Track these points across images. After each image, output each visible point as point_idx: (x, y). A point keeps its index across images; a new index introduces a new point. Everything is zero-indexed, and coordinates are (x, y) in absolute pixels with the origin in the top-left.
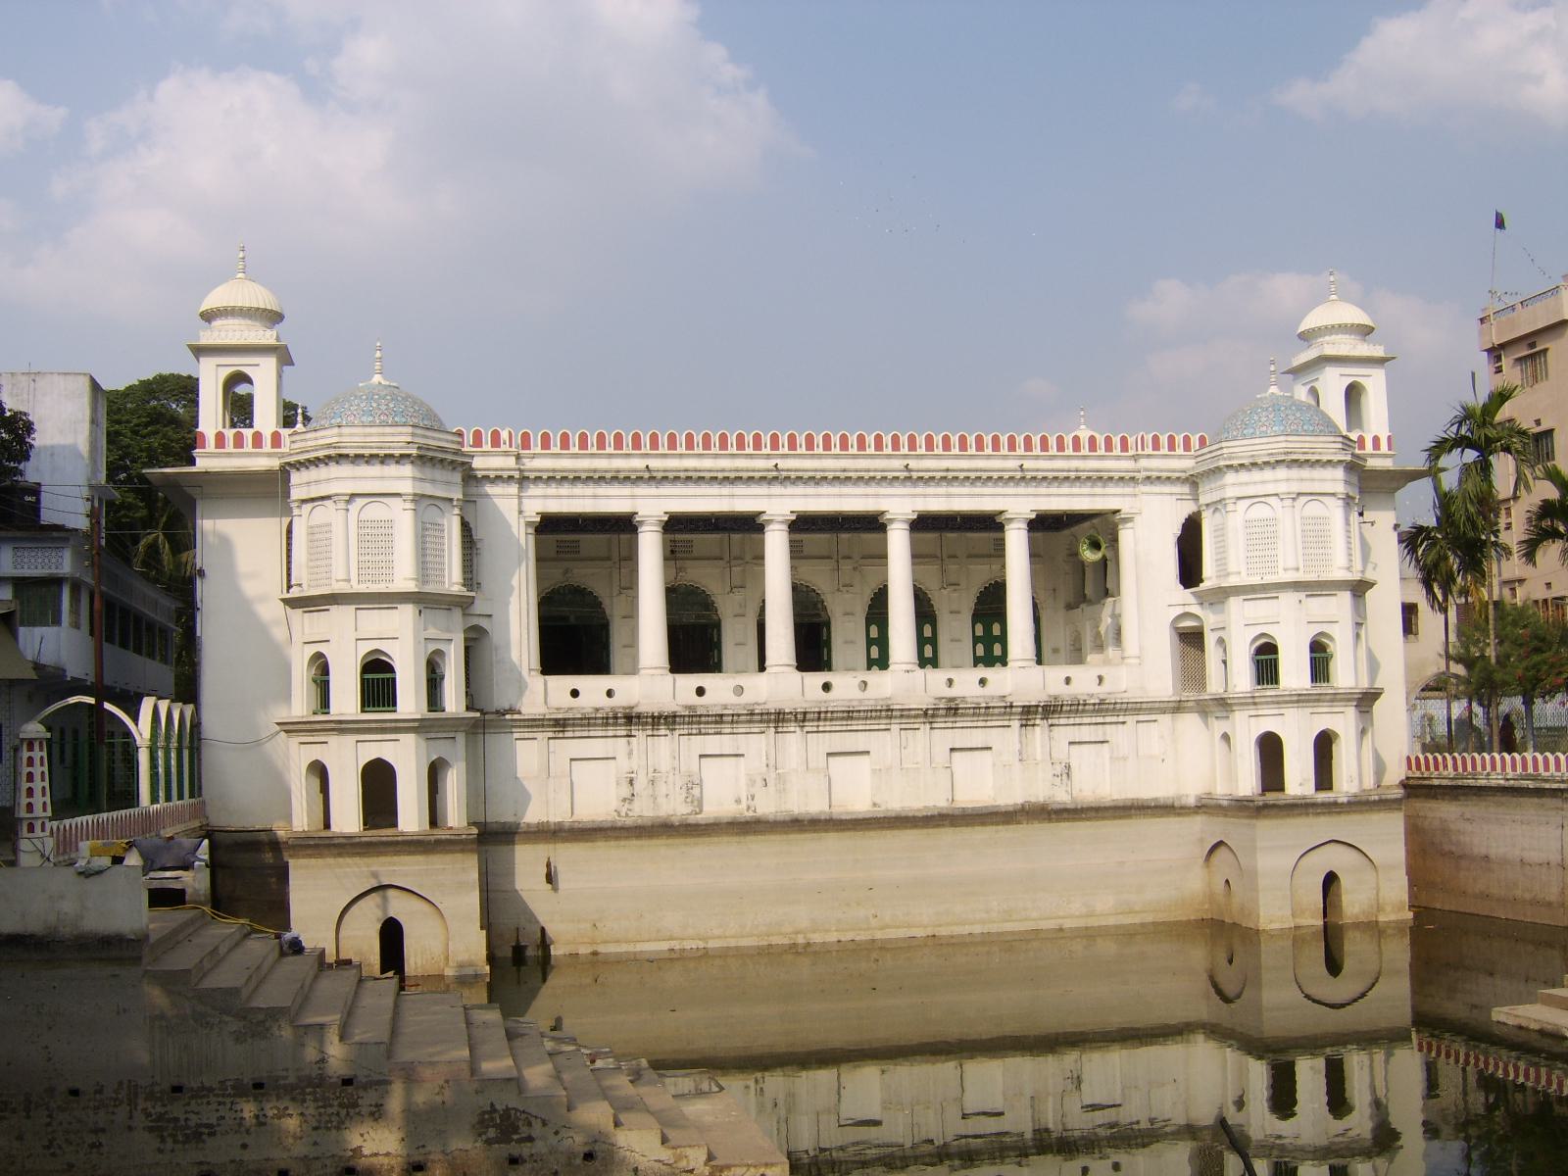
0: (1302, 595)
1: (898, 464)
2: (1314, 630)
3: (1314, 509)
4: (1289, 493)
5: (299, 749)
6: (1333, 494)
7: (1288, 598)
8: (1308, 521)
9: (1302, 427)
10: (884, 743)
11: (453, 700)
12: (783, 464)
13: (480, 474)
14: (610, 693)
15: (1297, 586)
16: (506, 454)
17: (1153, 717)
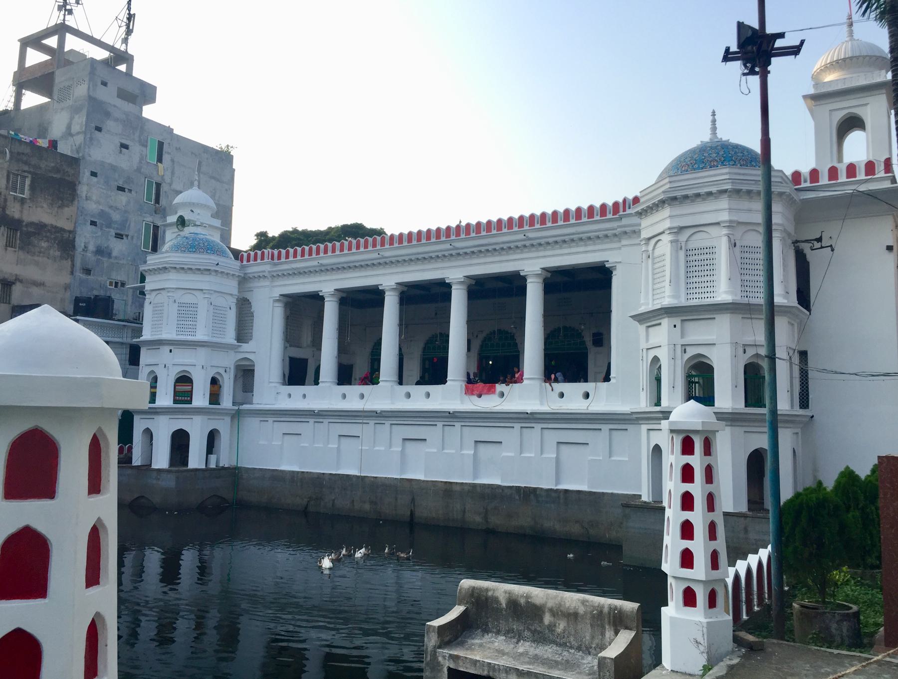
0: (677, 321)
1: (447, 246)
2: (691, 352)
3: (700, 240)
4: (669, 229)
5: (314, 426)
6: (718, 224)
7: (666, 322)
8: (746, 249)
9: (693, 166)
10: (433, 433)
11: (200, 399)
12: (387, 254)
13: (251, 276)
14: (304, 396)
15: (669, 311)
16: (265, 264)
17: (624, 427)
